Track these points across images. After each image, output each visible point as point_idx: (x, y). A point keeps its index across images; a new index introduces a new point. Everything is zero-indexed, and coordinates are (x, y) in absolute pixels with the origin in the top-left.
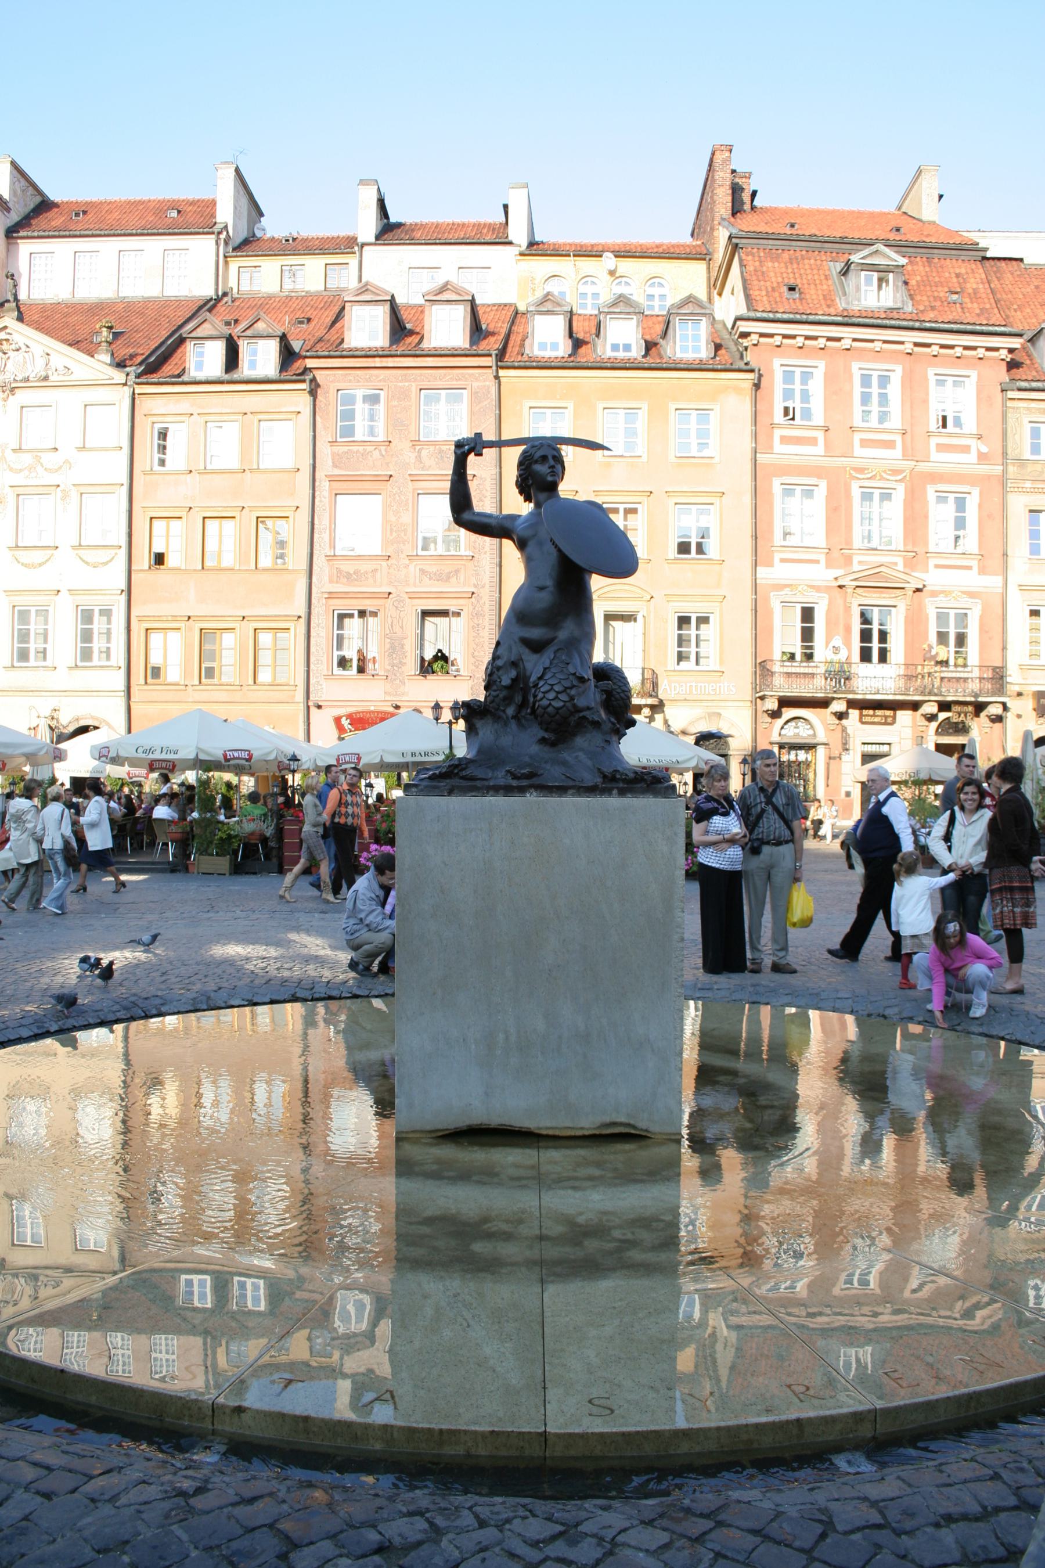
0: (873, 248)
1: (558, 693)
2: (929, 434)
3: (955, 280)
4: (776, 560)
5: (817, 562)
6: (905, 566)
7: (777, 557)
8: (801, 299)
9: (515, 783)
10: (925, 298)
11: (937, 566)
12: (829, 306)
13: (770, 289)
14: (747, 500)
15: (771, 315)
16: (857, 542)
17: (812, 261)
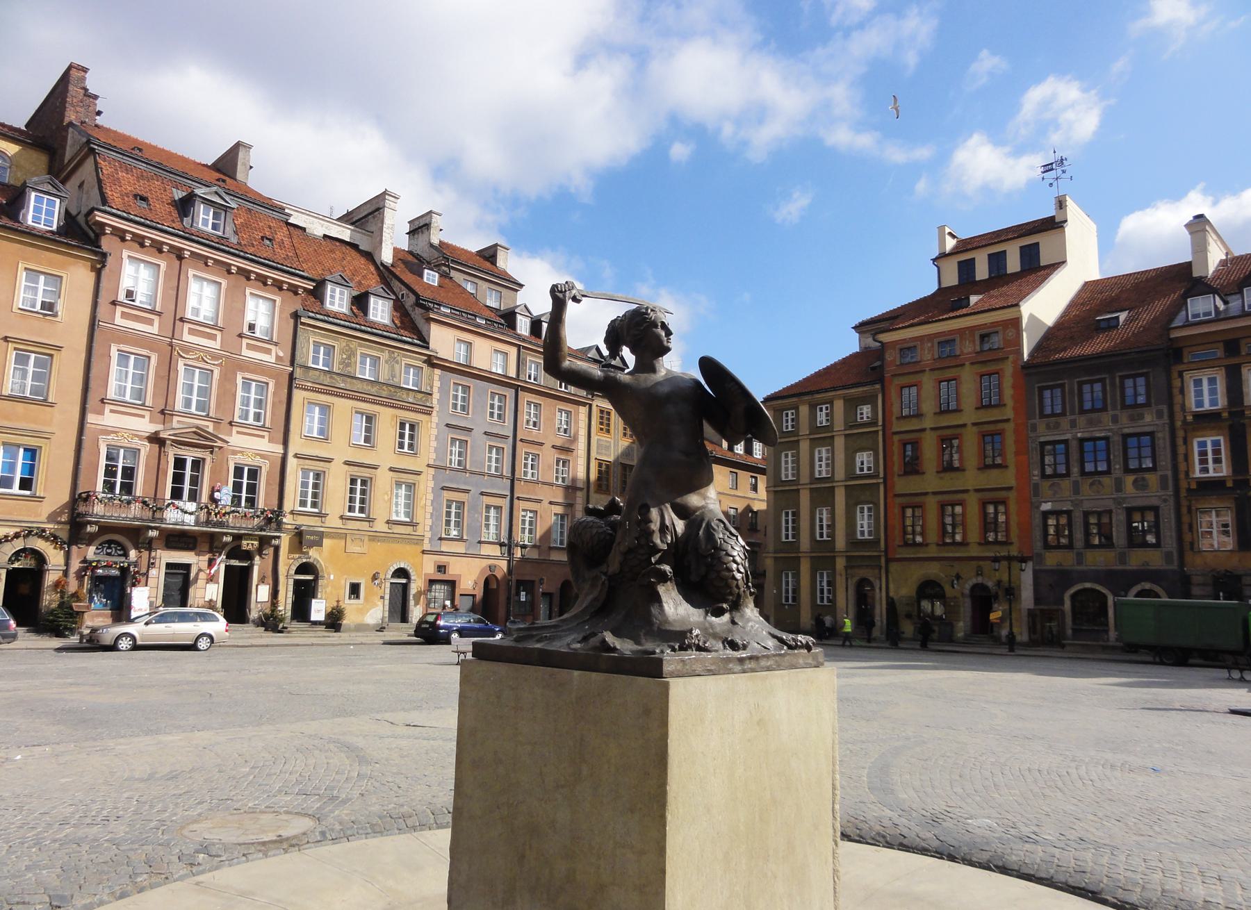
0: (215, 188)
2: (240, 336)
4: (107, 410)
5: (143, 416)
7: (108, 408)
11: (238, 432)
14: (83, 356)
16: (179, 406)
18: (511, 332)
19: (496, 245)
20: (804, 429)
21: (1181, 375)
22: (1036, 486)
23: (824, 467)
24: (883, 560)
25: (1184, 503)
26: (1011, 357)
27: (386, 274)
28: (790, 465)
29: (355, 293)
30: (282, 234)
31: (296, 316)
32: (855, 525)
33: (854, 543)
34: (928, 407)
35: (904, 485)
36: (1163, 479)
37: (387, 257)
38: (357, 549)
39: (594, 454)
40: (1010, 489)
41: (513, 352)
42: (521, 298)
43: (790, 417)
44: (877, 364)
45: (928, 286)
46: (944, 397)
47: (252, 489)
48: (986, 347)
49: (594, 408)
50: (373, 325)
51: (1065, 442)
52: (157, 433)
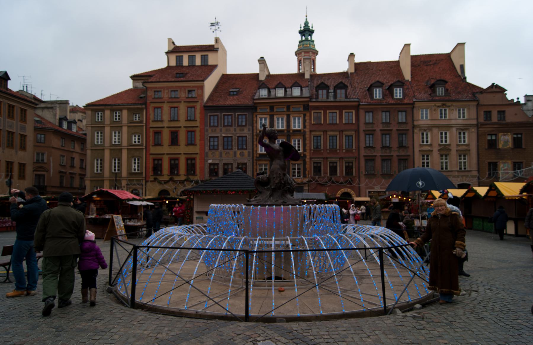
20: (107, 121)
21: (256, 117)
22: (207, 153)
23: (117, 140)
24: (144, 181)
25: (255, 162)
26: (200, 101)
28: (99, 137)
32: (132, 166)
33: (130, 174)
34: (166, 117)
35: (154, 150)
36: (249, 152)
40: (197, 154)
43: (100, 115)
44: (142, 96)
45: (164, 65)
46: (172, 114)
48: (190, 96)
51: (217, 137)
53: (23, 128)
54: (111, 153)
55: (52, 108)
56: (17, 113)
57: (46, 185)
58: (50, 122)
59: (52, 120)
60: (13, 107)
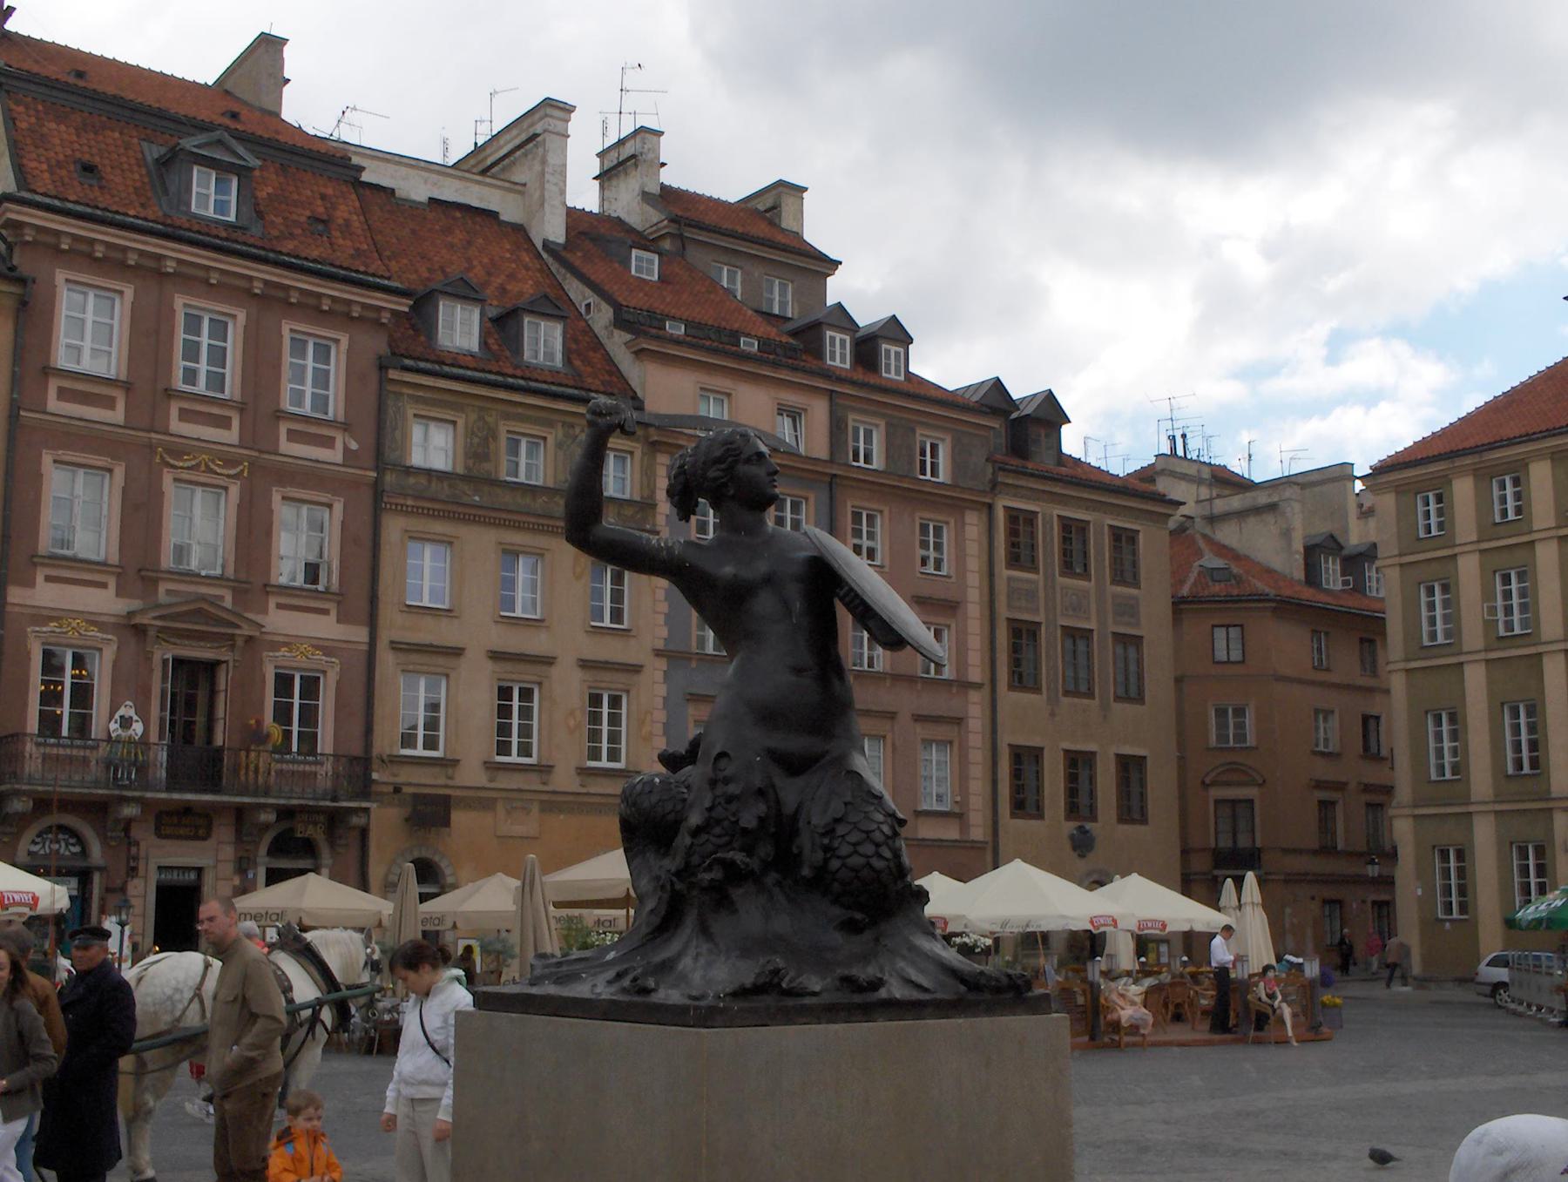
0: (217, 134)
1: (878, 845)
3: (319, 202)
4: (40, 579)
6: (234, 603)
8: (101, 188)
9: (857, 998)
10: (279, 220)
11: (280, 606)
12: (142, 205)
13: (53, 162)
15: (57, 203)
16: (167, 561)
17: (117, 135)
18: (813, 364)
19: (781, 184)
27: (554, 267)
29: (493, 312)
30: (346, 209)
31: (382, 368)
37: (554, 229)
38: (518, 830)
39: (1003, 612)
41: (819, 410)
42: (837, 289)
47: (309, 716)
49: (1000, 515)
50: (530, 373)
52: (131, 614)
53: (1129, 609)
54: (1490, 682)
55: (1272, 507)
56: (1100, 548)
57: (1258, 844)
58: (1270, 572)
59: (1277, 562)
60: (1083, 527)
